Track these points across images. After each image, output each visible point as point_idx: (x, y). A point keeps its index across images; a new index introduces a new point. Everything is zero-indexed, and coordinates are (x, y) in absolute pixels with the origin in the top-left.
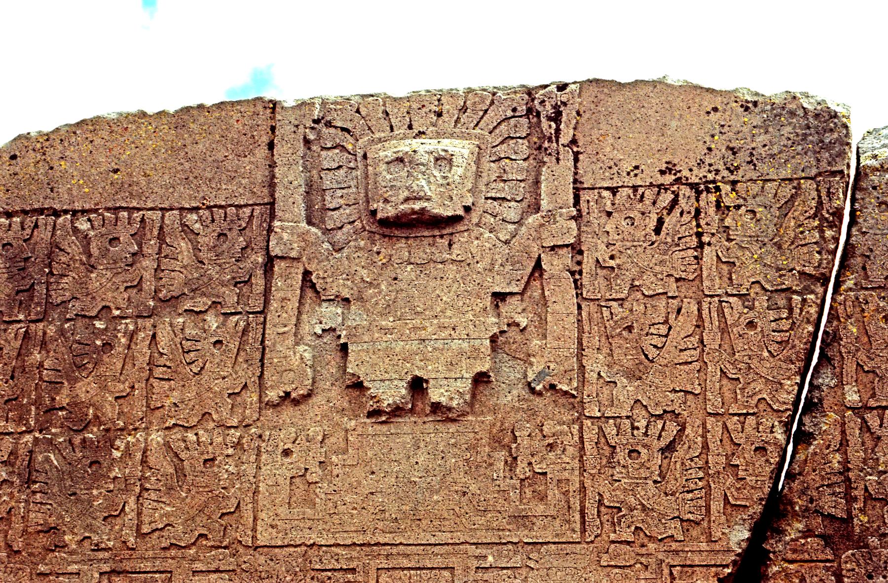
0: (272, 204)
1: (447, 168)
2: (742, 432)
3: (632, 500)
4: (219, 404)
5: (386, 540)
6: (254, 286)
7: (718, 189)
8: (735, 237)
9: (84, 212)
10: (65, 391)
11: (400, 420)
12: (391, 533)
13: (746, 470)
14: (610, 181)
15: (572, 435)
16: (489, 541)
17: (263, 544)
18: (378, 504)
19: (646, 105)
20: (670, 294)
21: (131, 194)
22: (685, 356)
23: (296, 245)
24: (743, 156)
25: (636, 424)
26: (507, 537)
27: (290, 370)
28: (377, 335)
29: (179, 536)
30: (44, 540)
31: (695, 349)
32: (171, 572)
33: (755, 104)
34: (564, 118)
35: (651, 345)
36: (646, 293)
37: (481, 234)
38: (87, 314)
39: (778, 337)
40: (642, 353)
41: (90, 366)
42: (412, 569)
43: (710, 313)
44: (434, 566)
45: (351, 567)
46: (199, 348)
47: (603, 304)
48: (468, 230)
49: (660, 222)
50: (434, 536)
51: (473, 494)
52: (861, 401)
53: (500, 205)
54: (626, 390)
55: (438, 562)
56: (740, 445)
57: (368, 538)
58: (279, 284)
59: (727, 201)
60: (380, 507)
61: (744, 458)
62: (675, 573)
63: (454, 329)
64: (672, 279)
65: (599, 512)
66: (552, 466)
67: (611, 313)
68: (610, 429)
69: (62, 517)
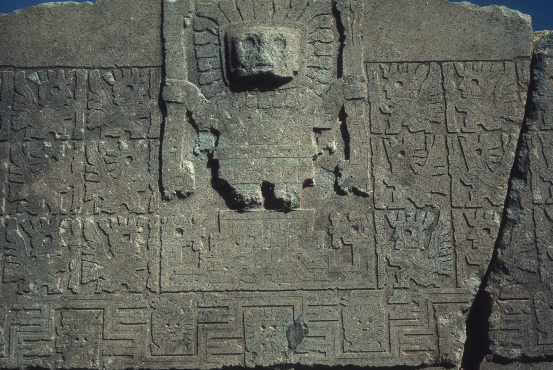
0: (163, 66)
1: (283, 46)
2: (475, 219)
3: (407, 261)
4: (132, 199)
5: (248, 288)
6: (152, 121)
8: (466, 96)
9: (34, 68)
10: (26, 188)
11: (254, 210)
12: (251, 283)
13: (478, 243)
14: (387, 58)
15: (368, 220)
16: (316, 288)
17: (165, 290)
18: (241, 264)
19: (407, 10)
20: (427, 132)
21: (66, 57)
22: (438, 171)
23: (181, 94)
25: (408, 214)
26: (327, 285)
27: (180, 176)
28: (238, 154)
29: (108, 285)
30: (14, 286)
31: (443, 166)
32: (103, 309)
35: (416, 163)
36: (412, 131)
37: (304, 90)
38: (38, 137)
40: (410, 169)
42: (266, 306)
43: (452, 144)
44: (280, 305)
45: (225, 305)
46: (116, 161)
47: (385, 137)
48: (296, 87)
50: (280, 285)
51: (304, 258)
52: (543, 200)
53: (316, 72)
54: (401, 192)
56: (473, 227)
57: (236, 286)
58: (170, 120)
60: (243, 267)
61: (477, 235)
62: (436, 307)
63: (289, 151)
64: (428, 122)
65: (386, 269)
66: (355, 240)
67: (390, 143)
68: (392, 217)
69: (26, 272)
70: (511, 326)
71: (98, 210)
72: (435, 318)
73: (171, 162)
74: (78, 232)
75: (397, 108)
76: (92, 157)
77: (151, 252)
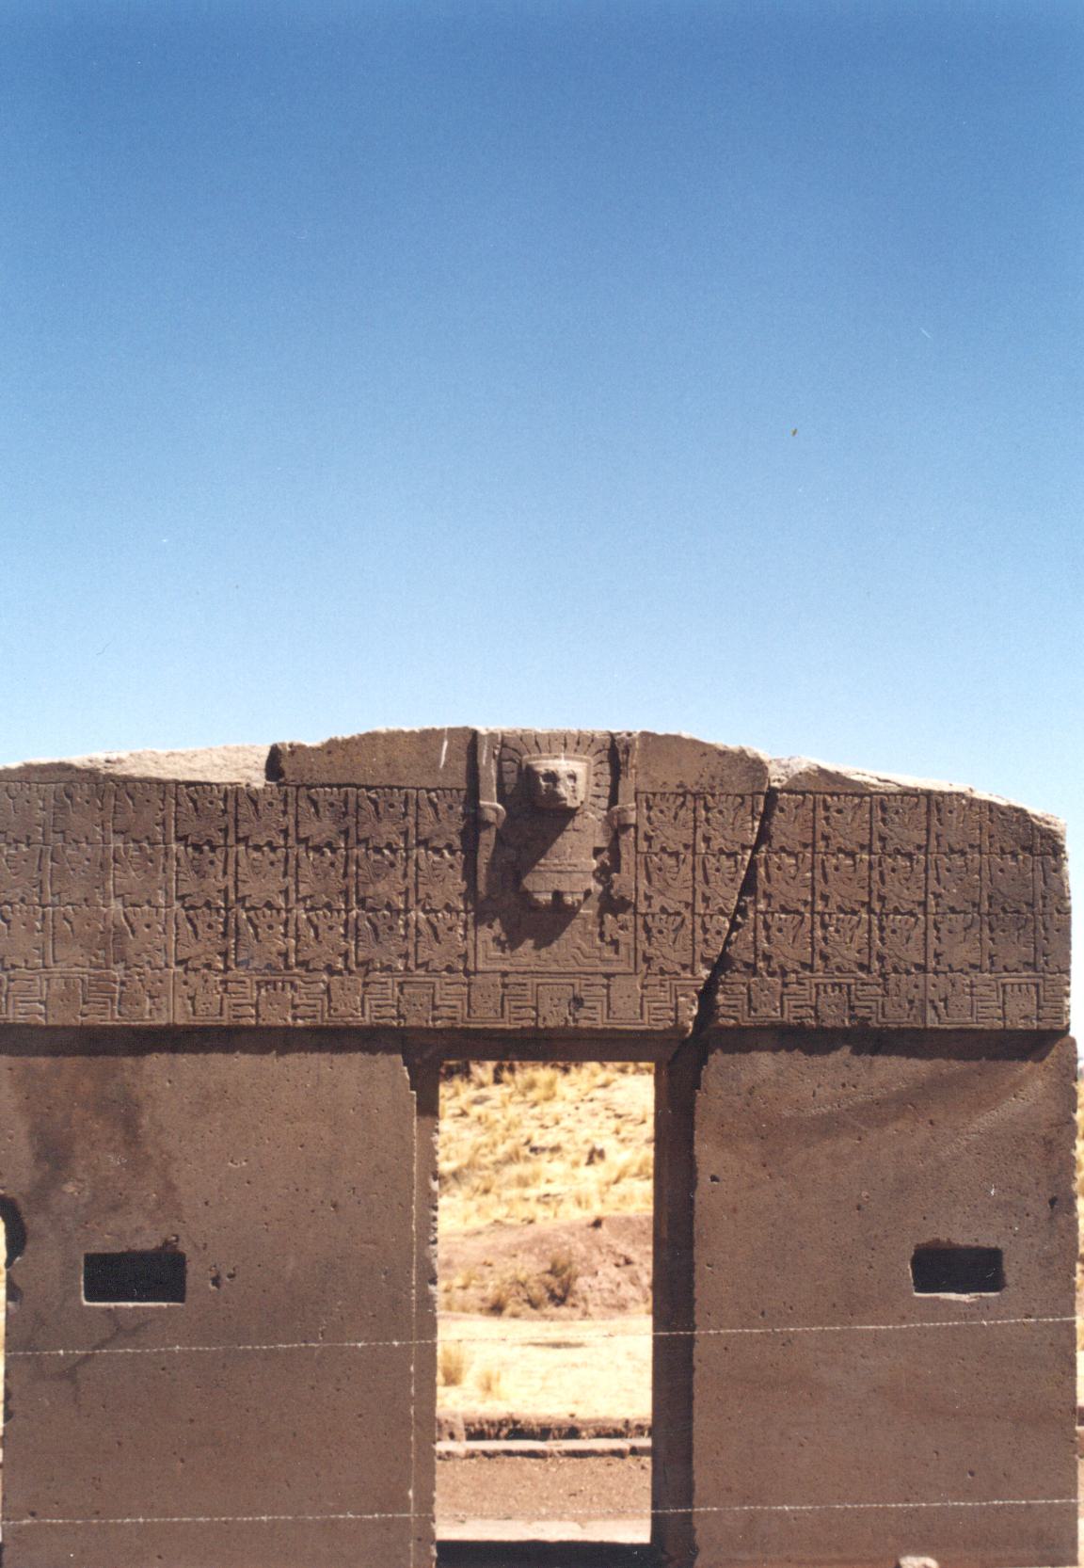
7: (705, 798)
17: (480, 970)
22: (686, 884)
24: (718, 780)
41: (384, 875)
49: (676, 814)
68: (649, 919)
71: (428, 908)
72: (677, 997)
74: (413, 924)
76: (422, 864)
77: (470, 942)
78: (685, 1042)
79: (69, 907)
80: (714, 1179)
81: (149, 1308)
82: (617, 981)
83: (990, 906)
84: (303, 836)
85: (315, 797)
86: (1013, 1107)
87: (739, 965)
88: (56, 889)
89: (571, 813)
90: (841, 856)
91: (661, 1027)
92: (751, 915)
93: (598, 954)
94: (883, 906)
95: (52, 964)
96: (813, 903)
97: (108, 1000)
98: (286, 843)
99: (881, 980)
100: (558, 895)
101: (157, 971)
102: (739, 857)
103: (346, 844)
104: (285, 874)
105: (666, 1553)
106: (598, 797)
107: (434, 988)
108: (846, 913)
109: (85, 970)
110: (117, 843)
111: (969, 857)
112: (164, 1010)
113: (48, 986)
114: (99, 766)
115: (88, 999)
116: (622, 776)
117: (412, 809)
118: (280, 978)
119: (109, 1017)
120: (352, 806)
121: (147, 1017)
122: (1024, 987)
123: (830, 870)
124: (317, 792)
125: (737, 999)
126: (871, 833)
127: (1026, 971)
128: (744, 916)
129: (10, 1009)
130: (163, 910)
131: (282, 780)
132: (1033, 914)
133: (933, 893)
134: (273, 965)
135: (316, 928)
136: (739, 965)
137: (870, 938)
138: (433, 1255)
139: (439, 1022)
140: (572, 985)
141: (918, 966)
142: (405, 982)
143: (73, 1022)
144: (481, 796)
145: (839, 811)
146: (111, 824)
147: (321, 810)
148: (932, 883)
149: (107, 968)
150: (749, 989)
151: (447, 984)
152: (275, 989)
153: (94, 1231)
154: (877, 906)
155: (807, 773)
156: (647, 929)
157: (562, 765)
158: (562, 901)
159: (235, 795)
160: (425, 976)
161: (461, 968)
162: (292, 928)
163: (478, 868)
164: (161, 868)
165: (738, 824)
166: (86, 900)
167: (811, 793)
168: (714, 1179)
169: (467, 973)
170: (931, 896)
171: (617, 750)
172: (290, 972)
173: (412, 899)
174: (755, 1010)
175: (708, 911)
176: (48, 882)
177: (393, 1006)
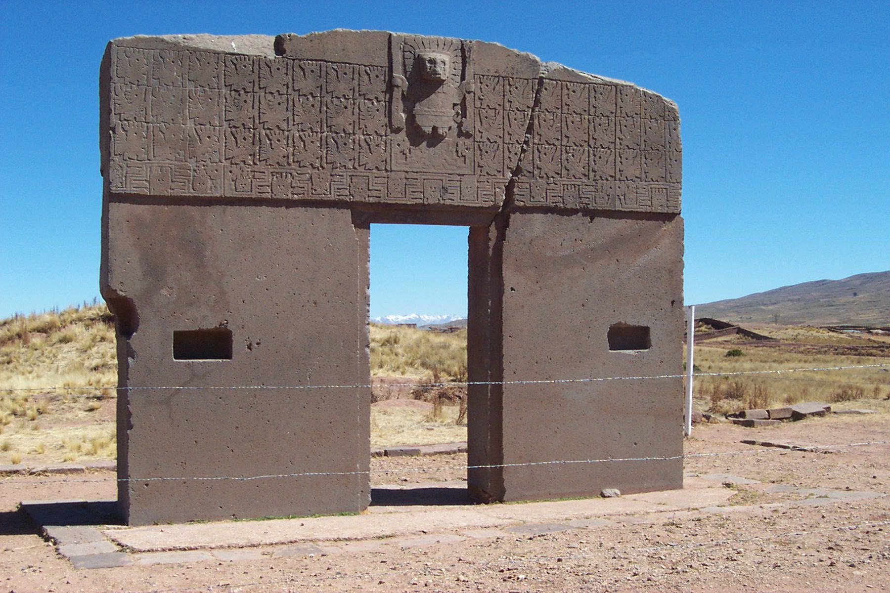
9: (335, 63)
33: (519, 55)
34: (472, 52)
39: (521, 123)
49: (495, 87)
55: (439, 178)
59: (511, 84)
70: (522, 193)
71: (365, 133)
72: (495, 189)
73: (396, 114)
74: (357, 142)
75: (485, 97)
78: (497, 215)
79: (163, 124)
80: (512, 289)
81: (211, 362)
82: (464, 178)
83: (645, 146)
84: (297, 89)
85: (303, 67)
86: (654, 252)
87: (525, 172)
88: (155, 113)
89: (441, 82)
90: (575, 115)
91: (486, 205)
92: (531, 145)
93: (455, 163)
94: (595, 144)
95: (153, 159)
96: (561, 140)
97: (186, 181)
98: (287, 92)
99: (594, 183)
100: (435, 129)
101: (215, 164)
102: (526, 113)
103: (321, 95)
104: (287, 110)
105: (487, 493)
106: (455, 75)
107: (368, 179)
108: (577, 146)
109: (172, 162)
110: (191, 87)
111: (636, 120)
112: (219, 187)
113: (151, 171)
114: (180, 41)
115: (174, 180)
116: (467, 64)
117: (356, 76)
118: (285, 171)
119: (187, 191)
120: (323, 73)
121: (209, 191)
122: (661, 189)
123: (570, 123)
124: (304, 63)
125: (524, 191)
126: (589, 104)
127: (662, 181)
128: (528, 145)
129: (128, 184)
130: (218, 128)
131: (284, 55)
132: (665, 151)
133: (619, 138)
134: (281, 163)
135: (304, 141)
136: (525, 172)
137: (589, 160)
138: (367, 331)
139: (371, 199)
140: (442, 180)
141: (611, 176)
142: (353, 176)
143: (166, 194)
144: (394, 71)
145: (574, 92)
146: (187, 76)
147: (306, 74)
148: (618, 132)
149: (186, 162)
150: (530, 187)
151: (375, 177)
152: (282, 177)
153: (179, 317)
154: (592, 142)
155: (558, 69)
156: (481, 150)
157: (439, 56)
158: (437, 132)
159: (258, 62)
160: (364, 172)
161: (384, 168)
162: (291, 141)
163: (392, 112)
164: (216, 103)
165: (525, 95)
166: (173, 120)
167: (560, 81)
168: (512, 289)
169: (386, 170)
170: (617, 139)
171: (464, 49)
172: (290, 167)
173: (357, 128)
174: (533, 197)
175: (511, 142)
176: (150, 109)
177: (346, 189)
